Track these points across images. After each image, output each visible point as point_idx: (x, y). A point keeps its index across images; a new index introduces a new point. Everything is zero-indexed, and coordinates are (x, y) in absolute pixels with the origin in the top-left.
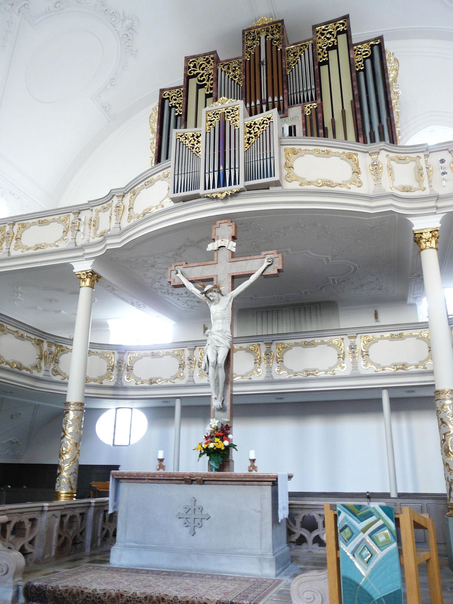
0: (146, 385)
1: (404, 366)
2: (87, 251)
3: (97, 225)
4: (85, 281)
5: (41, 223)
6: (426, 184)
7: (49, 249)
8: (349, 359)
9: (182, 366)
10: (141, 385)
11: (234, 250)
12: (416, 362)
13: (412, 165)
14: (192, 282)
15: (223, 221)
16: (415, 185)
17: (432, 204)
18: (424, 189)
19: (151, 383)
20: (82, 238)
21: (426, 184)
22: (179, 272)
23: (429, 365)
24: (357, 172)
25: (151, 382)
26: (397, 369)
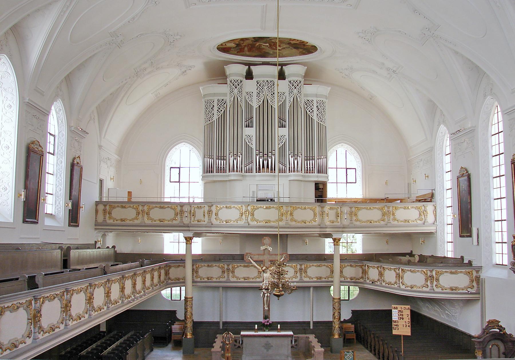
0: (206, 280)
1: (321, 278)
2: (191, 229)
3: (195, 215)
4: (189, 242)
5: (161, 208)
6: (339, 220)
7: (166, 222)
8: (298, 275)
9: (223, 272)
10: (203, 280)
11: (271, 251)
12: (325, 276)
13: (335, 211)
14: (254, 261)
15: (267, 237)
16: (335, 220)
17: (341, 230)
18: (339, 222)
19: (208, 280)
20: (186, 220)
21: (339, 220)
22: (250, 257)
23: (330, 279)
24: (315, 215)
25: (208, 278)
26: (318, 279)
